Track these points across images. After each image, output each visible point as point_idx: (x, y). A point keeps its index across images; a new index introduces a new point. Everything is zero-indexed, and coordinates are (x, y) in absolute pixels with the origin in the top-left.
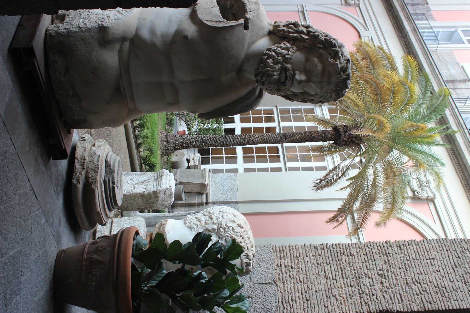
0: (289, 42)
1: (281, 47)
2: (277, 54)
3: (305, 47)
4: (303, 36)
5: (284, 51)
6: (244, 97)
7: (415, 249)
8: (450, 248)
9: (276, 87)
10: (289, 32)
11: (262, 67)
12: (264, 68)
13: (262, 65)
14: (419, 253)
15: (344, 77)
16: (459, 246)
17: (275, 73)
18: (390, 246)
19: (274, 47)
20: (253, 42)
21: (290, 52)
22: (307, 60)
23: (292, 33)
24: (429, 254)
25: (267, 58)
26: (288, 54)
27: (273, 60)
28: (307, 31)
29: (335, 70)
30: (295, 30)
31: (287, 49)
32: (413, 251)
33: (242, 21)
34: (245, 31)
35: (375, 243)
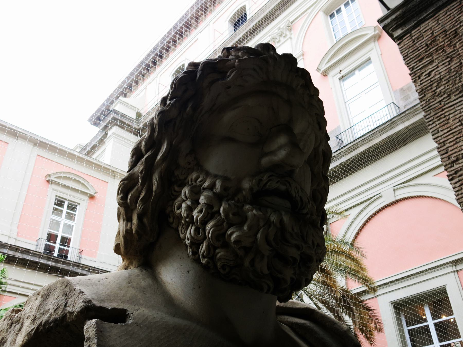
2: (211, 212)
4: (159, 158)
5: (202, 199)
7: (452, 144)
8: (437, 108)
11: (252, 262)
13: (247, 262)
14: (457, 138)
16: (431, 101)
17: (273, 218)
18: (456, 173)
20: (169, 301)
21: (206, 184)
22: (230, 140)
24: (454, 127)
25: (226, 245)
26: (212, 187)
28: (147, 152)
29: (254, 70)
30: (143, 185)
32: (456, 146)
33: (90, 327)
34: (130, 322)
35: (457, 194)
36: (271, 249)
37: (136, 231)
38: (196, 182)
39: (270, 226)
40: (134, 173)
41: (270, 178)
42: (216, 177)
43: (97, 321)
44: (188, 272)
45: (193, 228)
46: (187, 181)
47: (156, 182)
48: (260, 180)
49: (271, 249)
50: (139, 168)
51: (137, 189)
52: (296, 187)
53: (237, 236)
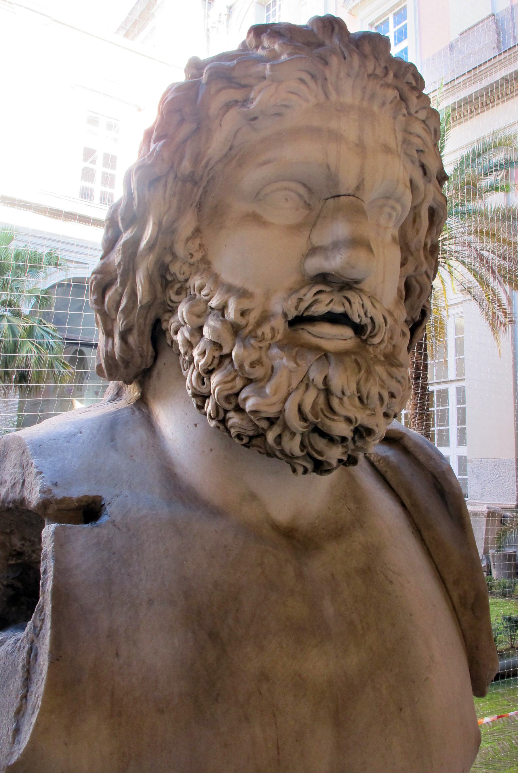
0: (173, 311)
1: (190, 345)
3: (197, 231)
4: (143, 244)
5: (206, 331)
6: (403, 505)
9: (380, 370)
10: (128, 312)
11: (279, 438)
12: (285, 427)
15: (336, 41)
19: (191, 377)
21: (213, 303)
22: (255, 219)
23: (133, 293)
25: (239, 409)
27: (249, 381)
28: (126, 229)
29: (302, 80)
30: (123, 284)
31: (201, 314)
34: (104, 519)
36: (306, 425)
37: (120, 356)
38: (200, 292)
39: (307, 387)
40: (110, 263)
41: (316, 298)
42: (230, 289)
43: (56, 528)
44: (196, 425)
45: (195, 374)
46: (187, 285)
47: (140, 287)
48: (300, 300)
49: (306, 425)
50: (116, 257)
51: (116, 290)
52: (363, 306)
53: (253, 405)
